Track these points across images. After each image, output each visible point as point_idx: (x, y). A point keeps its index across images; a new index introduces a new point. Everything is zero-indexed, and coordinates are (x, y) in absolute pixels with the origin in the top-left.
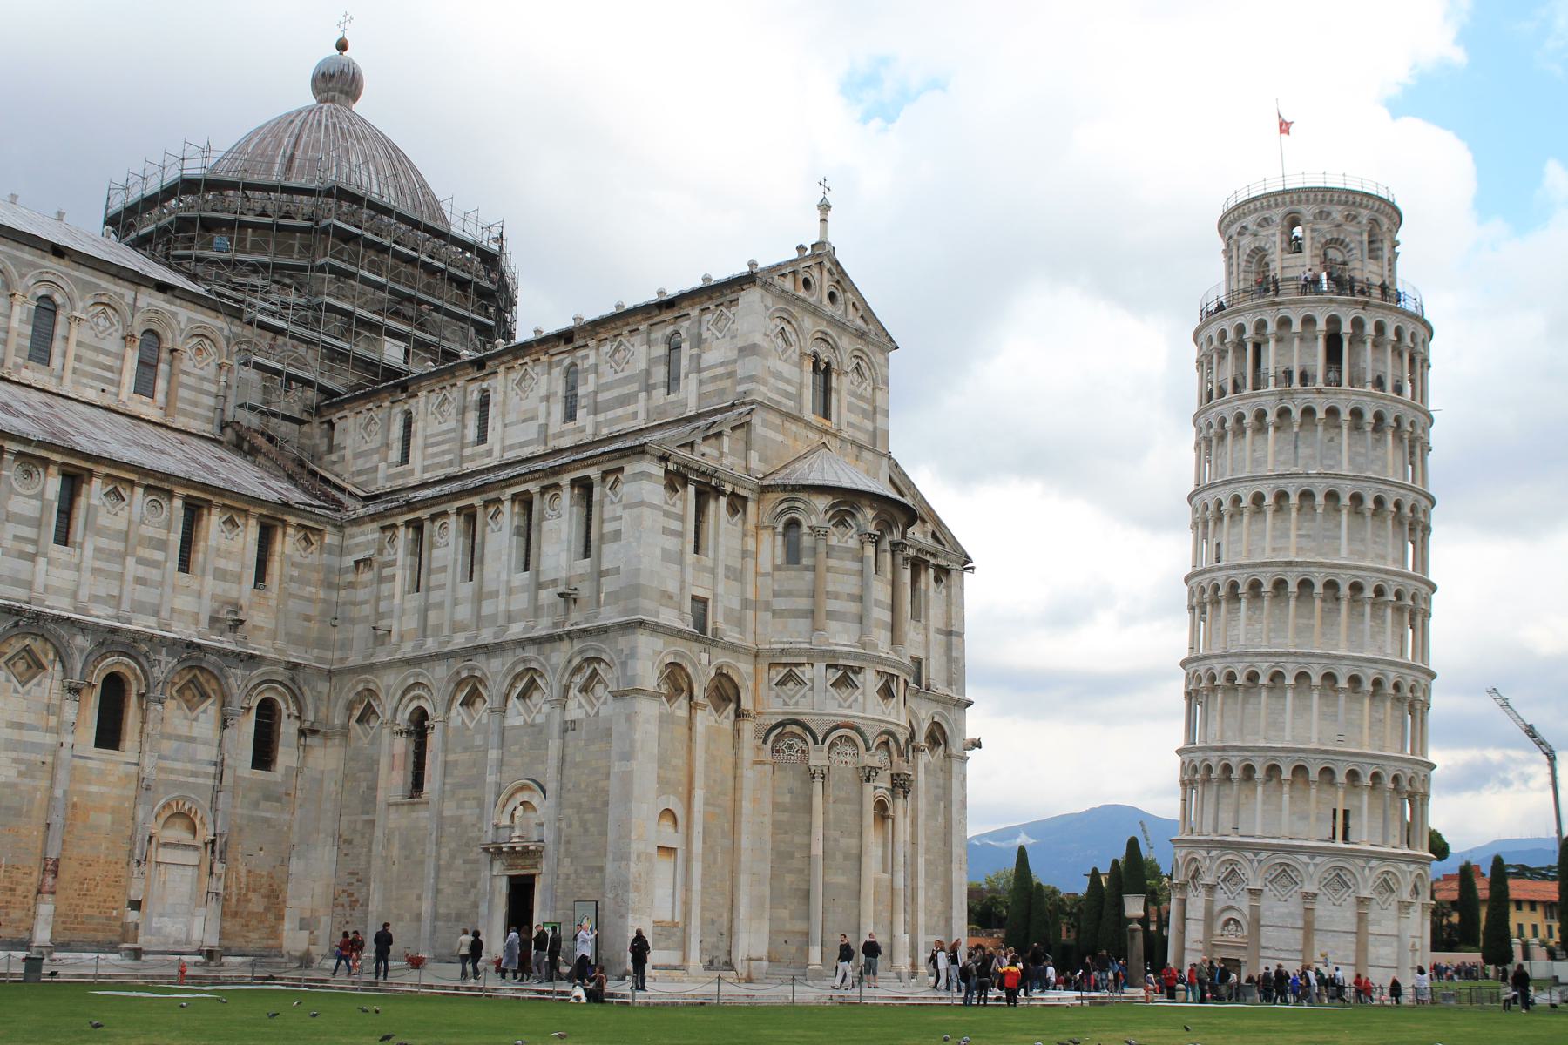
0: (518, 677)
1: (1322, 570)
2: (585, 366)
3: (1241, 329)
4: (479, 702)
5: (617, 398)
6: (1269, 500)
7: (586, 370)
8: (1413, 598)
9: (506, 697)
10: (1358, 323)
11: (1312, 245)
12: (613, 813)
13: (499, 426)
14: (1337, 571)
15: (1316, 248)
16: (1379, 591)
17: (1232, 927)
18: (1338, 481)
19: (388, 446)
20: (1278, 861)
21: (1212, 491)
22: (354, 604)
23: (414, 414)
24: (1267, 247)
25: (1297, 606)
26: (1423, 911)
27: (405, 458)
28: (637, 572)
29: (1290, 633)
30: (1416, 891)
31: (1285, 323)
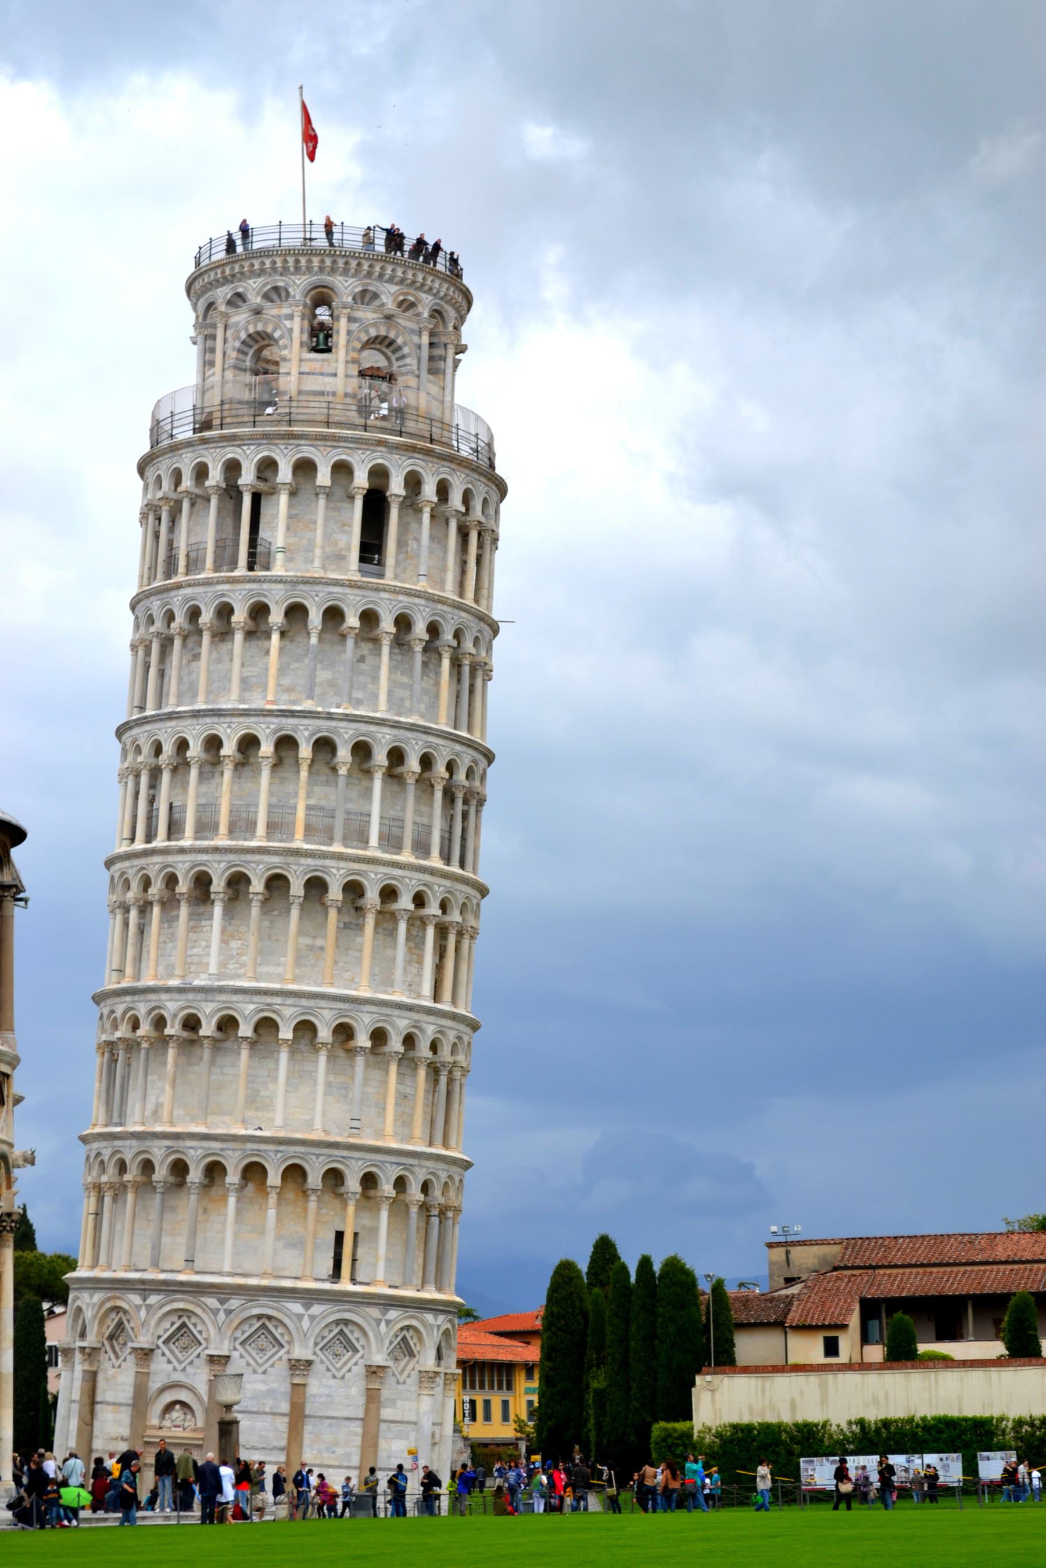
1: (342, 864)
3: (233, 468)
6: (267, 748)
10: (413, 482)
11: (348, 341)
14: (363, 867)
15: (354, 349)
17: (177, 1414)
18: (373, 728)
20: (255, 1311)
21: (173, 723)
24: (277, 335)
25: (300, 918)
26: (445, 1384)
29: (289, 959)
30: (439, 1357)
31: (305, 468)
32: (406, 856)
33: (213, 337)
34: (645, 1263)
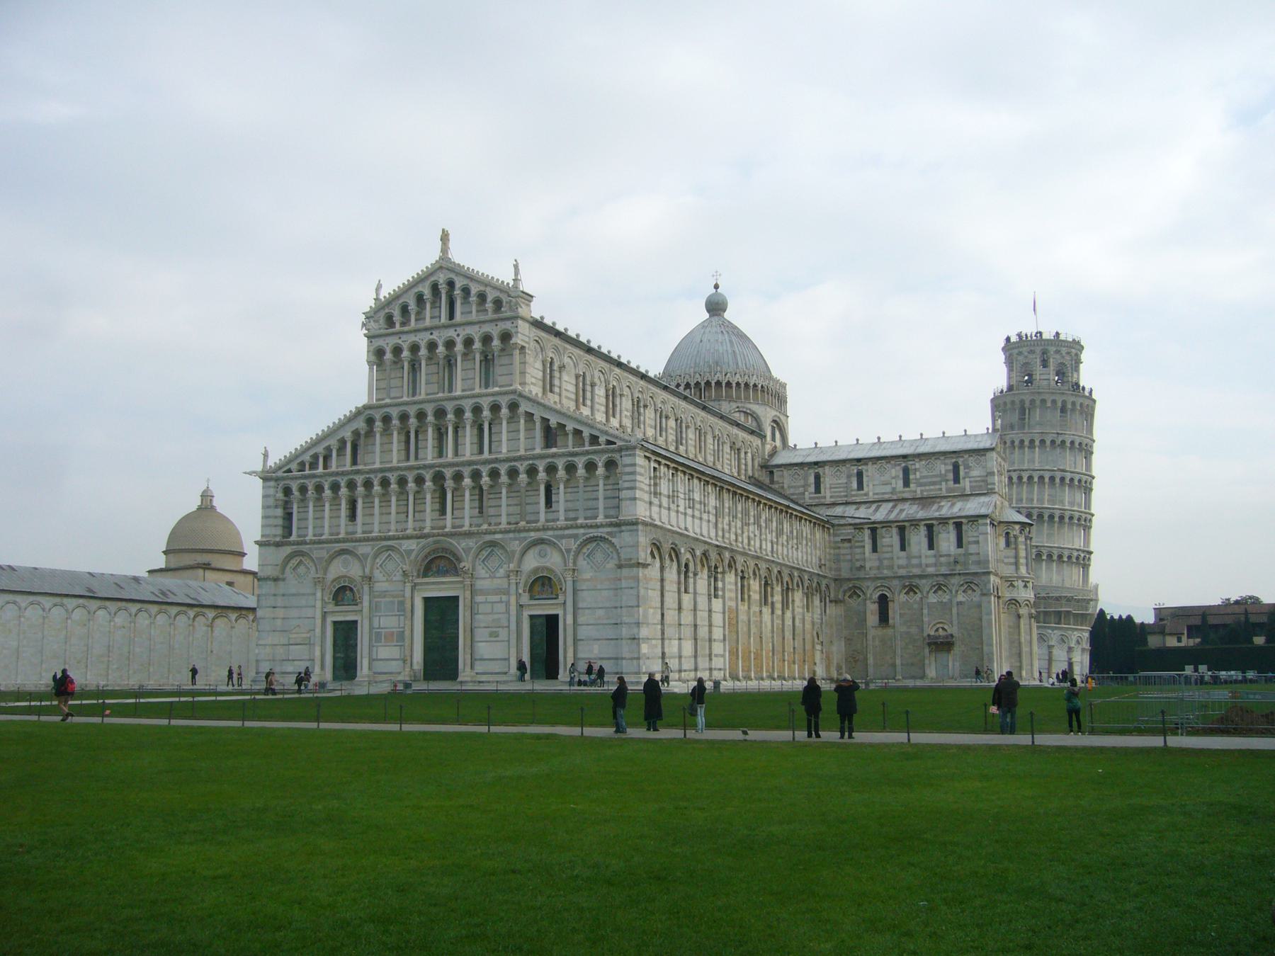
0: (934, 586)
2: (913, 467)
3: (1022, 402)
4: (911, 594)
5: (930, 482)
6: (1036, 479)
7: (915, 470)
8: (1085, 520)
9: (928, 592)
12: (985, 632)
13: (871, 486)
16: (1079, 519)
19: (810, 486)
22: (843, 555)
23: (821, 474)
27: (818, 490)
28: (988, 555)
30: (1087, 644)
32: (1075, 508)
33: (1012, 363)
34: (1120, 617)
